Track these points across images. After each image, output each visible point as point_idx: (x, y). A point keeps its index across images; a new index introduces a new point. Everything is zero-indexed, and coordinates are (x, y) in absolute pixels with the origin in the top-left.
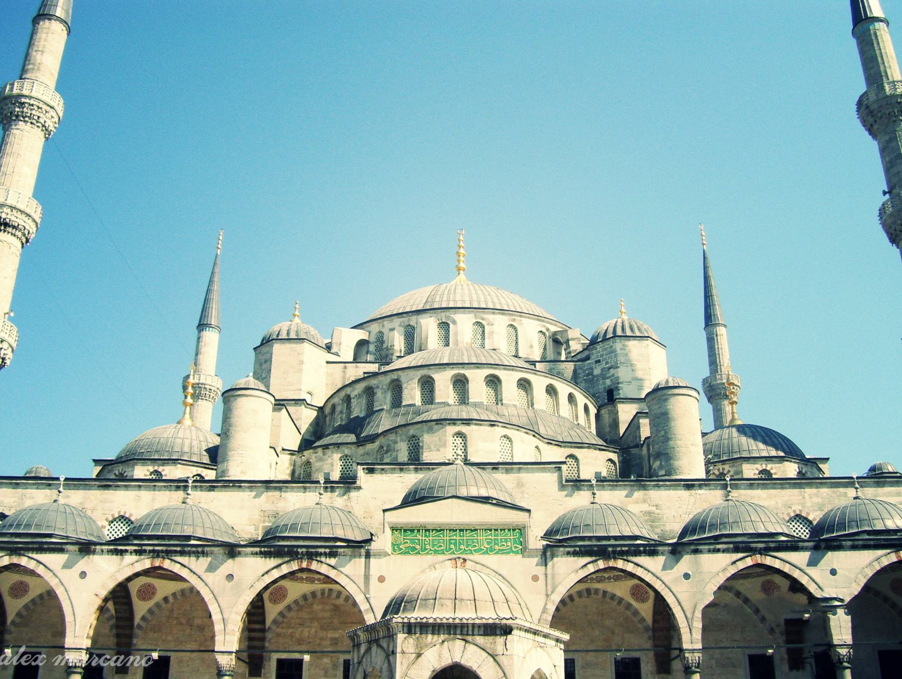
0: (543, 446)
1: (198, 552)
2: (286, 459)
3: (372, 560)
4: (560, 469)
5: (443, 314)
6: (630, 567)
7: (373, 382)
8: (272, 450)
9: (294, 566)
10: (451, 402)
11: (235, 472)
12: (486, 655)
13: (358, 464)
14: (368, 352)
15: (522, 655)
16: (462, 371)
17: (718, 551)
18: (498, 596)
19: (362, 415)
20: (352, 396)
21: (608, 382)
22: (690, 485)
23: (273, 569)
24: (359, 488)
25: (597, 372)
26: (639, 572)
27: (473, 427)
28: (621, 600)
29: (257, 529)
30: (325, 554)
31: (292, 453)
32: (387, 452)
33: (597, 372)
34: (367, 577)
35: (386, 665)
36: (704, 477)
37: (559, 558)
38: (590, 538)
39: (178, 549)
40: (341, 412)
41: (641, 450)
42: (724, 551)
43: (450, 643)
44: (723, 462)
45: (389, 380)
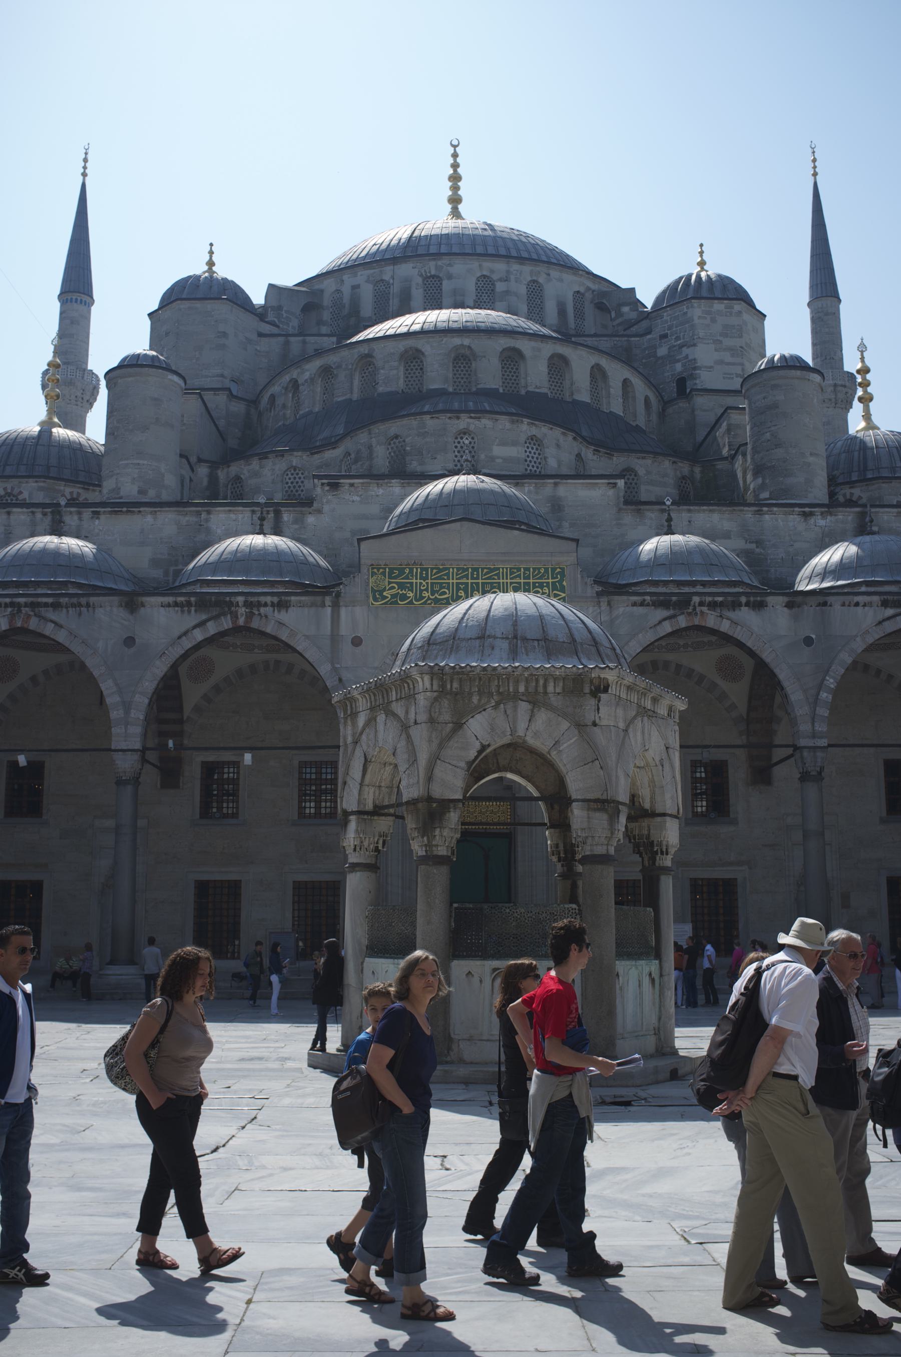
0: (588, 453)
1: (80, 605)
2: (203, 471)
3: (343, 611)
4: (615, 484)
5: (432, 264)
6: (725, 626)
7: (332, 359)
8: (184, 461)
9: (226, 623)
10: (451, 390)
11: (130, 490)
12: (565, 725)
13: (315, 477)
14: (320, 322)
15: (622, 725)
16: (466, 342)
17: (857, 604)
18: (580, 635)
19: (317, 410)
20: (300, 382)
21: (679, 367)
22: (807, 511)
23: (195, 627)
24: (319, 511)
25: (662, 351)
26: (738, 634)
27: (486, 422)
28: (702, 678)
29: (166, 573)
30: (273, 605)
31: (214, 465)
32: (356, 461)
33: (662, 351)
34: (335, 638)
35: (402, 743)
36: (826, 501)
37: (621, 610)
38: (666, 583)
39: (50, 600)
40: (284, 406)
41: (732, 464)
42: (865, 605)
43: (510, 705)
44: (852, 484)
45: (356, 356)
